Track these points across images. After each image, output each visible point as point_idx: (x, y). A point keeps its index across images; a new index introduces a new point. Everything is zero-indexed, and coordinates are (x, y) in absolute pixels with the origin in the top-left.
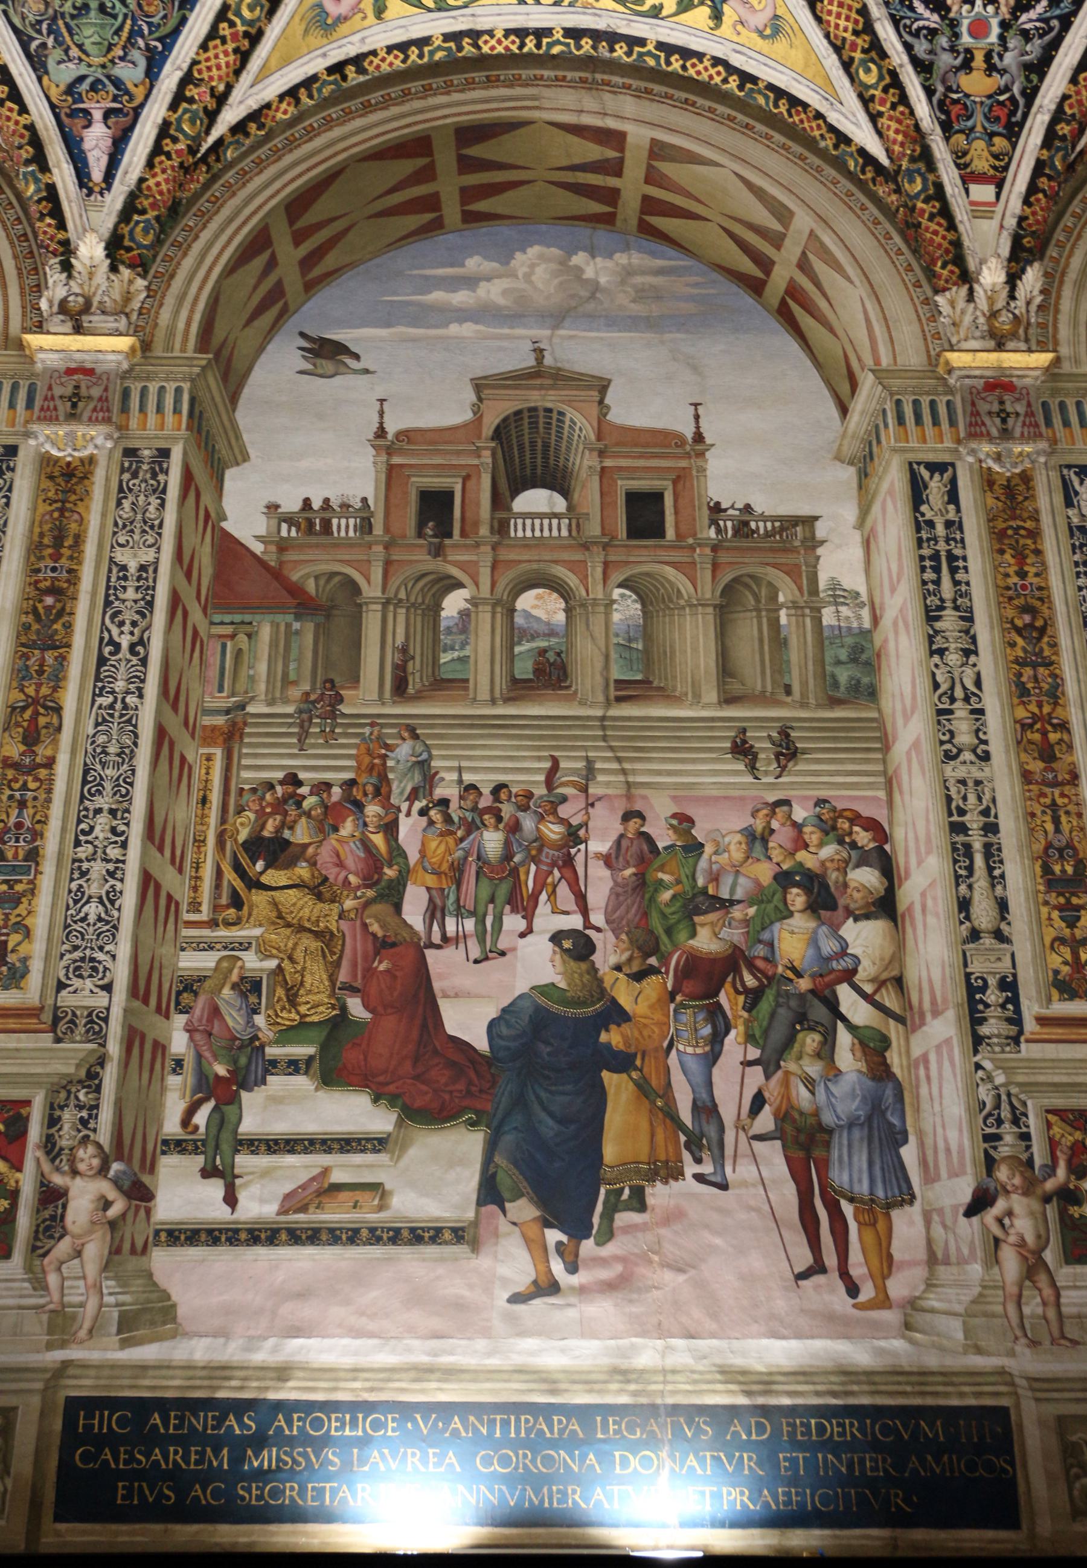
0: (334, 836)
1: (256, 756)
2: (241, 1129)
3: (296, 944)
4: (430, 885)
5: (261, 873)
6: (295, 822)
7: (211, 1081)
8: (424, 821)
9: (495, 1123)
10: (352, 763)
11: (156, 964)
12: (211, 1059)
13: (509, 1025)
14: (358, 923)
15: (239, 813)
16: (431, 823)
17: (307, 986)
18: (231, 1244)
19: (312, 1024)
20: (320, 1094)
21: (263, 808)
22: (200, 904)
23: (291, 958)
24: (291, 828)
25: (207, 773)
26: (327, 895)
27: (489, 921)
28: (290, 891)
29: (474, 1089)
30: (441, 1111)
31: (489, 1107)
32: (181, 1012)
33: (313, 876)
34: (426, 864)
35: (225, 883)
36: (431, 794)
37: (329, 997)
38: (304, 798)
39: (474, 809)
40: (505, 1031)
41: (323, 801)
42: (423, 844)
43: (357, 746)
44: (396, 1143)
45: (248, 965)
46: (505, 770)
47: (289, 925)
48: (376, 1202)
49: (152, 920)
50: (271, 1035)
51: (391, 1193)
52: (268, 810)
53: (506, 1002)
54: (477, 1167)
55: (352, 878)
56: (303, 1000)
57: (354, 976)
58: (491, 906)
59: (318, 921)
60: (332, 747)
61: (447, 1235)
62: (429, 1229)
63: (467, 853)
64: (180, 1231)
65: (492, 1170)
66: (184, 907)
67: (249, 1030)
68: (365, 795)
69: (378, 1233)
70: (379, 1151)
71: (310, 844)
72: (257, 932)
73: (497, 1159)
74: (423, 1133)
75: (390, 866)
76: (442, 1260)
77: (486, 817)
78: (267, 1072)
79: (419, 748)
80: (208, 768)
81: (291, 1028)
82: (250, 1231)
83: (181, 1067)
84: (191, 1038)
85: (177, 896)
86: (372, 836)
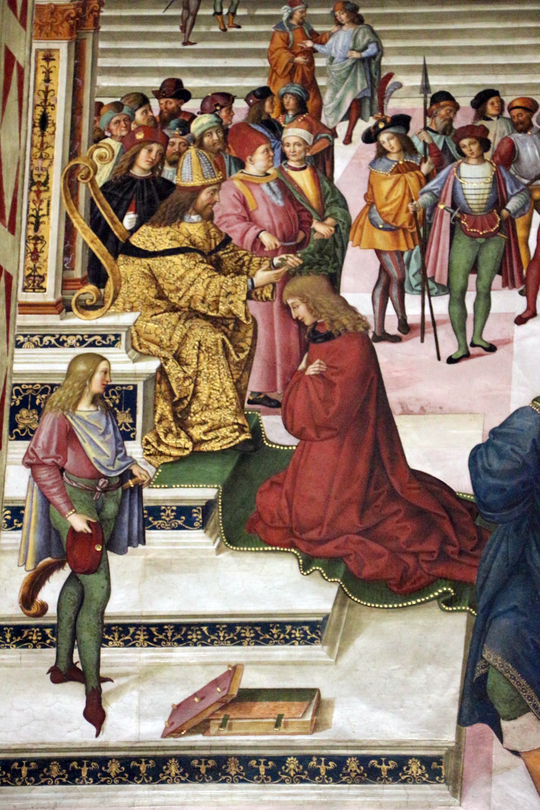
0: (238, 174)
1: (119, 53)
2: (110, 610)
3: (185, 337)
4: (382, 246)
5: (132, 232)
6: (180, 154)
7: (65, 539)
10: (264, 63)
12: (64, 507)
13: (501, 456)
14: (276, 304)
16: (382, 153)
17: (203, 397)
18: (96, 781)
19: (211, 454)
20: (226, 557)
21: (131, 134)
22: (43, 278)
23: (177, 357)
25: (47, 80)
26: (229, 264)
28: (175, 259)
29: (451, 549)
31: (474, 577)
32: (19, 438)
33: (208, 234)
34: (376, 216)
35: (79, 247)
36: (382, 109)
37: (236, 414)
39: (447, 130)
40: (496, 464)
41: (220, 122)
43: (271, 37)
44: (337, 629)
45: (116, 368)
46: (494, 69)
47: (174, 309)
48: (308, 717)
50: (151, 470)
51: (330, 704)
52: (140, 136)
53: (496, 421)
54: (458, 665)
55: (266, 239)
56: (197, 418)
57: (272, 383)
58: (473, 278)
59: (217, 302)
60: (232, 38)
61: (415, 768)
62: (389, 758)
63: (437, 199)
64: (20, 761)
65: (479, 672)
66: (19, 282)
67: (118, 464)
68: (284, 111)
69: (313, 763)
70: (312, 641)
71: (204, 187)
72: (128, 319)
73: (488, 654)
74: (376, 614)
75: (322, 220)
77: (465, 142)
78: (146, 525)
79: (363, 38)
80: (48, 72)
81: (181, 460)
82: (125, 761)
83: (20, 518)
84: (34, 476)
86: (294, 175)
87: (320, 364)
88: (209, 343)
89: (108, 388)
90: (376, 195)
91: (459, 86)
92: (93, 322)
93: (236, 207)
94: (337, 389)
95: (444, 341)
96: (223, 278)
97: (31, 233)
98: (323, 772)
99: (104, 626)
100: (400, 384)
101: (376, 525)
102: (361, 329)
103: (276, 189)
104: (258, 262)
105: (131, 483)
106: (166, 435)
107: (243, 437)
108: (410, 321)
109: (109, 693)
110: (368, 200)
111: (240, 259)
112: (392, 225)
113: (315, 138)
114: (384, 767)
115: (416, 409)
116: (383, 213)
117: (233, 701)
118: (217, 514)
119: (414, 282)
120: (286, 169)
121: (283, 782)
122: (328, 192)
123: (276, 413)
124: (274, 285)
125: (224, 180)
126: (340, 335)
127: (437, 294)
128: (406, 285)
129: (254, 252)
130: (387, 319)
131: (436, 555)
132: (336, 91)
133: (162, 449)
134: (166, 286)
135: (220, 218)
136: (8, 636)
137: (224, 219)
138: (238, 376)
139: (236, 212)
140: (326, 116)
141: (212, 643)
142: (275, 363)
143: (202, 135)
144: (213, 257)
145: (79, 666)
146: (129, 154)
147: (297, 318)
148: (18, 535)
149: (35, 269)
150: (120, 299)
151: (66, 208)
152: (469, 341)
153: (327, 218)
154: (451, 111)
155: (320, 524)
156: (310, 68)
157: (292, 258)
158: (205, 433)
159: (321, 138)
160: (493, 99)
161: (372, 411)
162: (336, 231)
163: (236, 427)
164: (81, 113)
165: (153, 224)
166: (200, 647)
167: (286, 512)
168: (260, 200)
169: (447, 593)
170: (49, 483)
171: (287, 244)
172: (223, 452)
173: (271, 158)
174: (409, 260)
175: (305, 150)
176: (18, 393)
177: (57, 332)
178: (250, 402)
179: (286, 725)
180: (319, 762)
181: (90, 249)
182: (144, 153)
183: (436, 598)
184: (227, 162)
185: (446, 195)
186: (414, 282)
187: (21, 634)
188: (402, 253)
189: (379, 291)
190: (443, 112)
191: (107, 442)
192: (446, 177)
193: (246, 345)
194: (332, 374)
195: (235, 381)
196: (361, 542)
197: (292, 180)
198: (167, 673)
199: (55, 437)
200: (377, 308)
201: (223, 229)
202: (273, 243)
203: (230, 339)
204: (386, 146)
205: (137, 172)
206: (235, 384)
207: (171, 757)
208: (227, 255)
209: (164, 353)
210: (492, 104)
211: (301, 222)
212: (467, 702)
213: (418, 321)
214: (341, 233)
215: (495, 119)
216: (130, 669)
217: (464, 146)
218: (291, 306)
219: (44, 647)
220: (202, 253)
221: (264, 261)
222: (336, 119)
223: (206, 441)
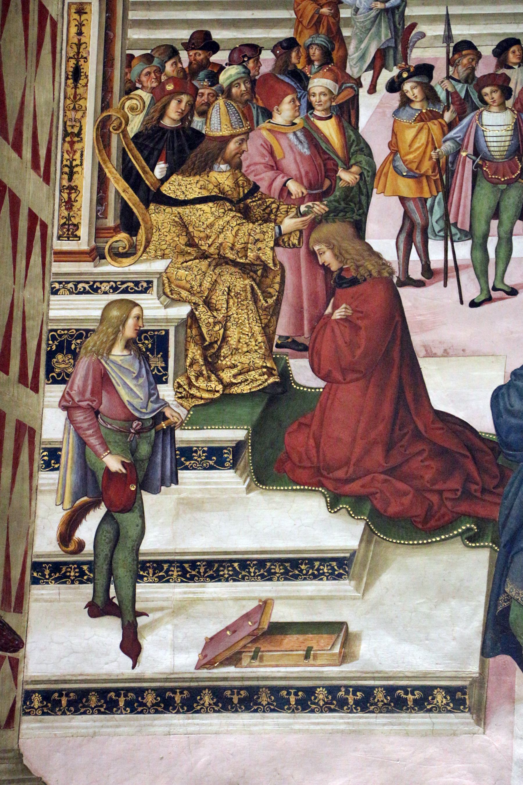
0: (264, 125)
2: (145, 547)
3: (215, 283)
4: (406, 193)
5: (163, 181)
6: (209, 104)
8: (395, 98)
9: (504, 539)
11: (17, 314)
12: (99, 448)
14: (303, 251)
15: (128, 92)
16: (406, 102)
17: (233, 342)
18: (133, 711)
19: (242, 396)
21: (162, 85)
22: (77, 226)
23: (207, 303)
24: (204, 114)
25: (80, 33)
26: (258, 212)
27: (492, 244)
28: (205, 207)
30: (425, 521)
31: (496, 514)
32: (55, 382)
33: (236, 183)
34: (399, 163)
36: (405, 58)
37: (264, 357)
38: (221, 68)
39: (469, 79)
40: (517, 405)
41: (247, 72)
42: (394, 134)
45: (147, 313)
47: (204, 256)
48: (337, 649)
49: (10, 252)
50: (183, 413)
51: (358, 636)
52: (170, 87)
54: (481, 600)
55: (293, 187)
56: (227, 362)
57: (299, 327)
58: (494, 223)
59: (245, 249)
61: (440, 698)
62: (415, 688)
63: (459, 146)
64: (60, 692)
65: (502, 605)
66: (54, 231)
67: (151, 406)
68: (310, 62)
69: (341, 693)
70: (339, 577)
71: (232, 136)
72: (160, 265)
73: (510, 588)
74: (402, 550)
75: (347, 168)
76: (434, 734)
77: (487, 90)
78: (178, 465)
80: (80, 25)
81: (212, 401)
82: (160, 692)
83: (58, 459)
84: (70, 418)
85: (43, 216)
86: (320, 124)
87: (346, 308)
88: (237, 289)
89: (140, 333)
90: (400, 144)
91: (480, 35)
92: (126, 269)
93: (263, 156)
94: (363, 333)
95: (466, 285)
96: (251, 225)
97: (65, 183)
98: (351, 701)
99: (139, 562)
100: (423, 328)
101: (400, 465)
102: (386, 274)
103: (302, 138)
104: (285, 209)
105: (164, 425)
106: (197, 378)
107: (271, 380)
108: (433, 266)
109: (145, 626)
110: (393, 148)
111: (268, 207)
112: (416, 173)
113: (340, 88)
114: (410, 697)
115: (440, 352)
116: (406, 160)
117: (264, 634)
118: (247, 454)
119: (437, 228)
120: (312, 119)
121: (313, 711)
122: (354, 141)
123: (302, 357)
124: (301, 232)
125: (251, 130)
126: (365, 280)
127: (460, 240)
128: (429, 230)
129: (282, 200)
130: (410, 264)
131: (459, 493)
132: (361, 41)
133: (193, 391)
134: (196, 234)
135: (248, 166)
136: (47, 572)
137: (252, 168)
138: (266, 321)
139: (263, 161)
140: (351, 66)
141: (243, 579)
142: (302, 308)
143: (230, 86)
144: (242, 205)
145: (115, 601)
146: (159, 105)
147: (323, 264)
148: (55, 475)
149: (69, 218)
150: (151, 247)
151: (99, 158)
152: (491, 286)
153: (352, 166)
154: (473, 60)
155: (347, 463)
156: (334, 18)
157: (319, 206)
158: (235, 376)
159: (346, 88)
160: (514, 48)
161: (396, 355)
162: (361, 179)
163: (265, 370)
164: (112, 66)
165: (183, 174)
166: (231, 583)
167: (314, 451)
168: (287, 150)
169: (469, 530)
170: (85, 425)
171: (314, 192)
172: (252, 394)
173: (297, 108)
174: (432, 207)
175: (331, 100)
176: (54, 338)
177: (91, 279)
178: (278, 346)
179: (315, 657)
180: (347, 692)
181: (122, 198)
182: (174, 104)
183: (460, 534)
184: (254, 112)
185: (468, 142)
186: (437, 228)
187: (60, 570)
188: (426, 200)
189: (402, 238)
190: (465, 61)
191: (140, 386)
192: (469, 125)
193: (273, 290)
194: (358, 319)
195: (263, 325)
196: (386, 481)
197: (317, 129)
198: (200, 608)
199: (90, 382)
200: (401, 254)
201: (251, 178)
202: (299, 191)
203: (257, 285)
204: (410, 95)
205: (167, 122)
206: (263, 328)
207: (205, 688)
208: (255, 203)
209: (194, 299)
210: (514, 52)
211: (326, 171)
212: (489, 635)
213: (441, 265)
214: (365, 181)
215: (516, 67)
216: (165, 604)
217: (486, 94)
218: (317, 252)
219: (81, 582)
220: (231, 201)
221: (291, 208)
222: (360, 69)
223: (236, 384)
